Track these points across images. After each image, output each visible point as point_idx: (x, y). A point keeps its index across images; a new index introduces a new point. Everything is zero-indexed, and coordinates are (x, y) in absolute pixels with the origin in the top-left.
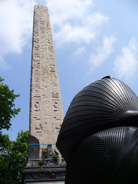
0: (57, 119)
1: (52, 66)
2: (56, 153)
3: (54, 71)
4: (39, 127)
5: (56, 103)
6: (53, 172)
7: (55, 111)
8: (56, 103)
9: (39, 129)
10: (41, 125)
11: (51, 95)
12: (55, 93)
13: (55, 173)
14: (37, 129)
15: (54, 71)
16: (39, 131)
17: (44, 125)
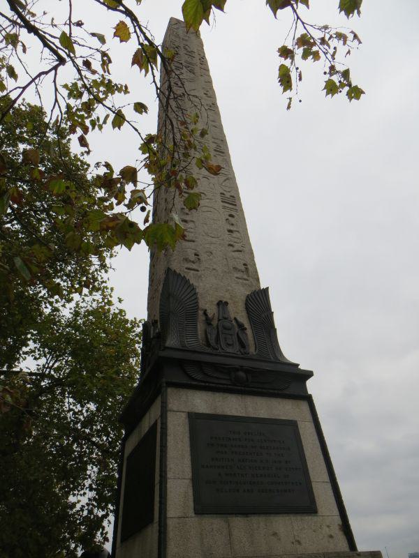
0: (235, 249)
1: (219, 142)
2: (241, 326)
3: (223, 153)
4: (192, 258)
5: (231, 216)
6: (242, 369)
7: (230, 231)
8: (231, 216)
9: (193, 262)
10: (198, 255)
11: (219, 198)
12: (228, 195)
13: (247, 371)
14: (186, 260)
15: (223, 153)
16: (194, 266)
17: (203, 257)
